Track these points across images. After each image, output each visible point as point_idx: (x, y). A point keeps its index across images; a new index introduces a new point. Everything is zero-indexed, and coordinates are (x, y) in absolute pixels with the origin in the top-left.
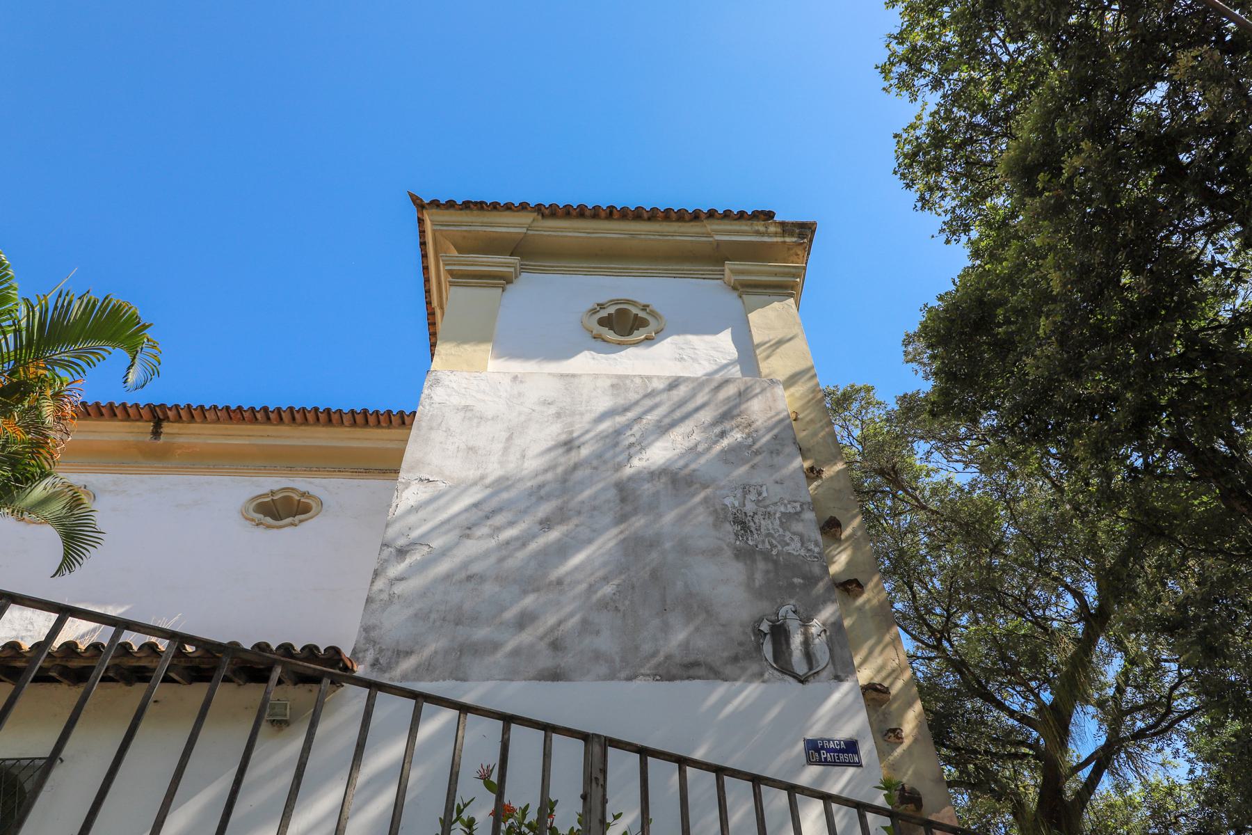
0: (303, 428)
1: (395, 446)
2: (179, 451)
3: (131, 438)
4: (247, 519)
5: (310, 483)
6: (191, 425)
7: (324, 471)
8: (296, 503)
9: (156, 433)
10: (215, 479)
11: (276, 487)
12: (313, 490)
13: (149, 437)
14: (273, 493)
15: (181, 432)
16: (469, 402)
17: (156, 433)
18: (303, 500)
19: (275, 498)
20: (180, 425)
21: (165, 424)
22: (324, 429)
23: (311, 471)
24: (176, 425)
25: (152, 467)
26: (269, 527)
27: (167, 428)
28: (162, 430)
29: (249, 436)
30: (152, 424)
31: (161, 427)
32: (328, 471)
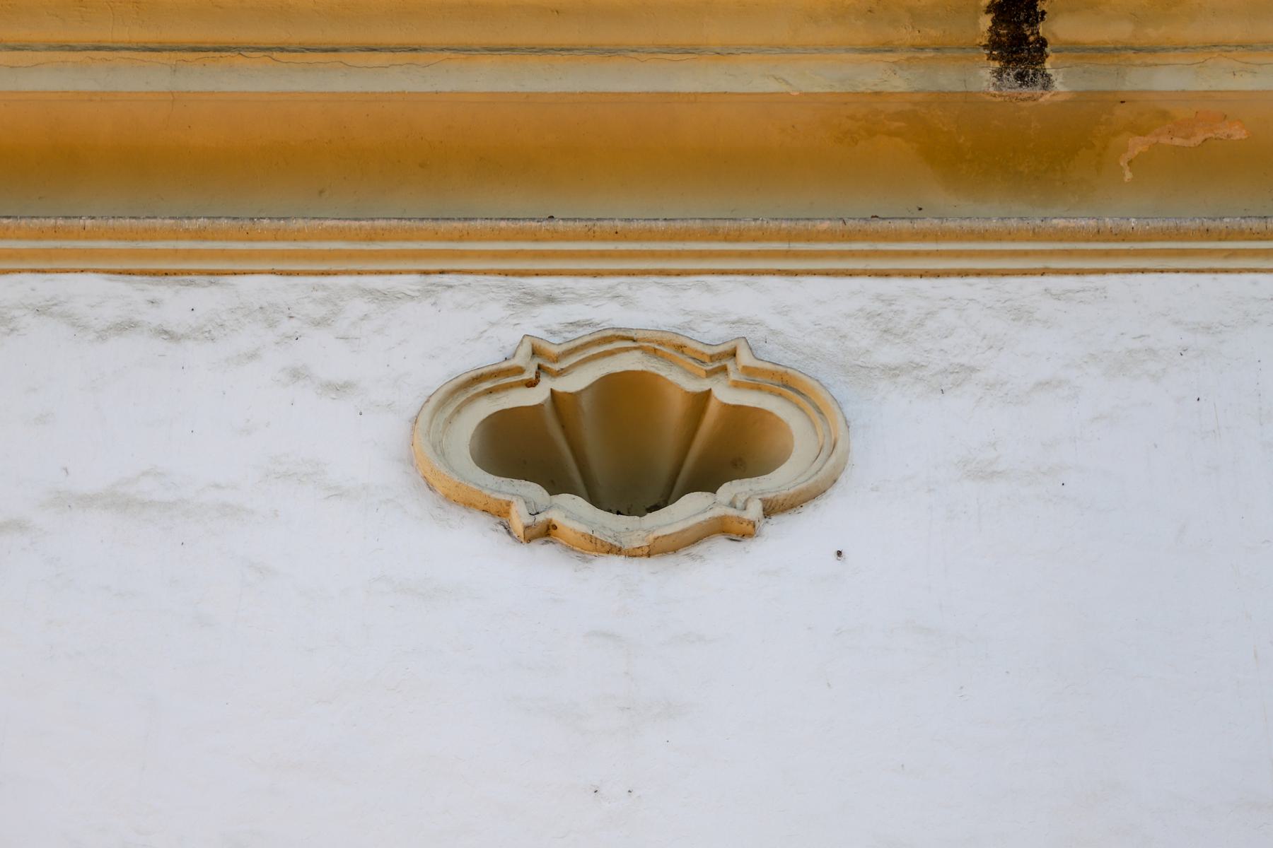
2: (1138, 145)
15: (1153, 34)
25: (1036, 235)
28: (1042, 29)
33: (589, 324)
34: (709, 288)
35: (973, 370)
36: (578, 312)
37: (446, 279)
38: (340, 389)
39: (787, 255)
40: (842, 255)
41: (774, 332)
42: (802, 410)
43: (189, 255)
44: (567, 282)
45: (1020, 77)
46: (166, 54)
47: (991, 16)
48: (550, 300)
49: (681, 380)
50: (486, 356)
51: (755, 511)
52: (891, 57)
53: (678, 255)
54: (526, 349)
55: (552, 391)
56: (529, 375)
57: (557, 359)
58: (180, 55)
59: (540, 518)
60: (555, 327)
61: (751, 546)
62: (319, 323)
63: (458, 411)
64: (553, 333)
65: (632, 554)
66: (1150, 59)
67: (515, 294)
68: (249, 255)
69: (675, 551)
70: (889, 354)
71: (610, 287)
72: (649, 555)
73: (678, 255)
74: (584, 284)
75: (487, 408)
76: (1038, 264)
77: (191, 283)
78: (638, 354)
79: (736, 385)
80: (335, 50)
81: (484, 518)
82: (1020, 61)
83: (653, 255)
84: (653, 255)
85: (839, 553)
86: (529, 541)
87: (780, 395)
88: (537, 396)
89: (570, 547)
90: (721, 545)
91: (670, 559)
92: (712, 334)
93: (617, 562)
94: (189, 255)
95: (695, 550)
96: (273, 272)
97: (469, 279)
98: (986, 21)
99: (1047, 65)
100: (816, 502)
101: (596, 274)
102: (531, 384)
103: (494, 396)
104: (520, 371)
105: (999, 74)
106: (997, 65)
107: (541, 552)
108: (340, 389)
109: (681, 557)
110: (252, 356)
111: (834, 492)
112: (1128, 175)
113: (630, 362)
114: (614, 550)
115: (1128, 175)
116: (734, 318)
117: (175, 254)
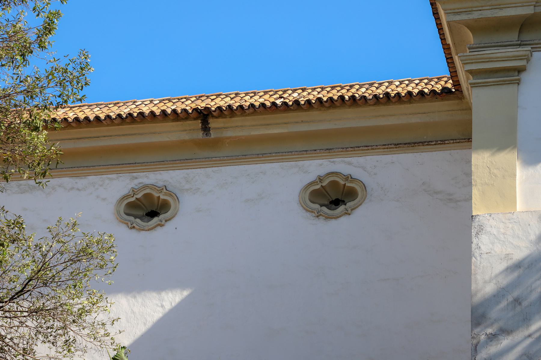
0: (331, 111)
1: (419, 121)
3: (185, 136)
4: (307, 210)
5: (350, 164)
6: (233, 119)
7: (358, 150)
8: (342, 186)
9: (206, 129)
10: (266, 167)
11: (322, 172)
12: (356, 173)
13: (200, 135)
14: (320, 179)
15: (227, 125)
16: (509, 251)
17: (206, 129)
18: (348, 184)
19: (324, 184)
20: (224, 120)
21: (211, 120)
22: (351, 110)
23: (348, 151)
24: (220, 120)
25: (210, 161)
26: (328, 218)
27: (213, 123)
28: (209, 126)
29: (285, 123)
30: (200, 121)
31: (208, 124)
32: (362, 150)
33: (142, 183)
34: (161, 174)
35: (199, 189)
36: (140, 180)
37: (121, 175)
38: (104, 199)
39: (172, 167)
40: (181, 166)
41: (170, 183)
42: (173, 199)
43: (81, 173)
44: (139, 174)
45: (206, 134)
46: (73, 140)
47: (201, 124)
48: (136, 178)
49: (156, 195)
50: (125, 192)
51: (164, 221)
52: (186, 132)
53: (156, 168)
54: (131, 191)
55: (136, 198)
56: (132, 195)
57: (136, 192)
58: (75, 140)
59: (132, 225)
60: (137, 184)
61: (164, 228)
62: (101, 186)
63: (122, 203)
64: (136, 185)
65: (146, 230)
66: (227, 129)
67: (131, 177)
68: (90, 173)
69: (152, 229)
70: (187, 186)
71: (146, 174)
72: (148, 230)
73: (156, 168)
74: (142, 174)
75: (126, 202)
76: (211, 166)
77: (82, 178)
78: (149, 189)
79: (163, 195)
80: (99, 137)
81: (125, 225)
82: (207, 131)
83: (152, 168)
84: (152, 168)
85: (176, 228)
86: (131, 229)
87: (170, 196)
88: (133, 199)
89: (137, 229)
90: (159, 227)
91: (151, 231)
92: (160, 184)
93: (144, 232)
94: (81, 173)
95: (155, 229)
96: (94, 175)
97: (124, 174)
98: (200, 125)
99: (211, 131)
100: (174, 218)
101: (144, 172)
102: (133, 197)
103: (127, 199)
104: (131, 195)
105: (203, 134)
106: (203, 132)
107: (133, 230)
108: (104, 199)
109: (153, 230)
110: (91, 194)
111: (176, 216)
112: (227, 145)
113: (148, 191)
114: (144, 230)
115: (227, 145)
116: (164, 180)
117: (79, 173)
